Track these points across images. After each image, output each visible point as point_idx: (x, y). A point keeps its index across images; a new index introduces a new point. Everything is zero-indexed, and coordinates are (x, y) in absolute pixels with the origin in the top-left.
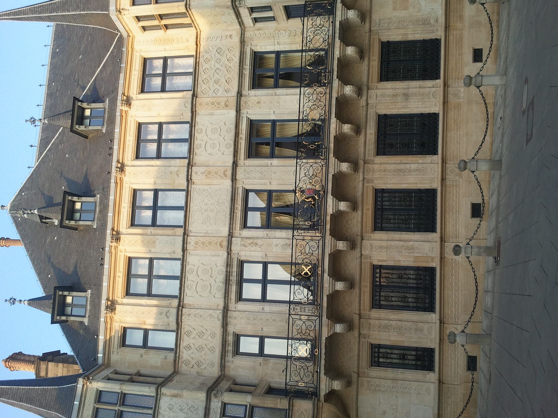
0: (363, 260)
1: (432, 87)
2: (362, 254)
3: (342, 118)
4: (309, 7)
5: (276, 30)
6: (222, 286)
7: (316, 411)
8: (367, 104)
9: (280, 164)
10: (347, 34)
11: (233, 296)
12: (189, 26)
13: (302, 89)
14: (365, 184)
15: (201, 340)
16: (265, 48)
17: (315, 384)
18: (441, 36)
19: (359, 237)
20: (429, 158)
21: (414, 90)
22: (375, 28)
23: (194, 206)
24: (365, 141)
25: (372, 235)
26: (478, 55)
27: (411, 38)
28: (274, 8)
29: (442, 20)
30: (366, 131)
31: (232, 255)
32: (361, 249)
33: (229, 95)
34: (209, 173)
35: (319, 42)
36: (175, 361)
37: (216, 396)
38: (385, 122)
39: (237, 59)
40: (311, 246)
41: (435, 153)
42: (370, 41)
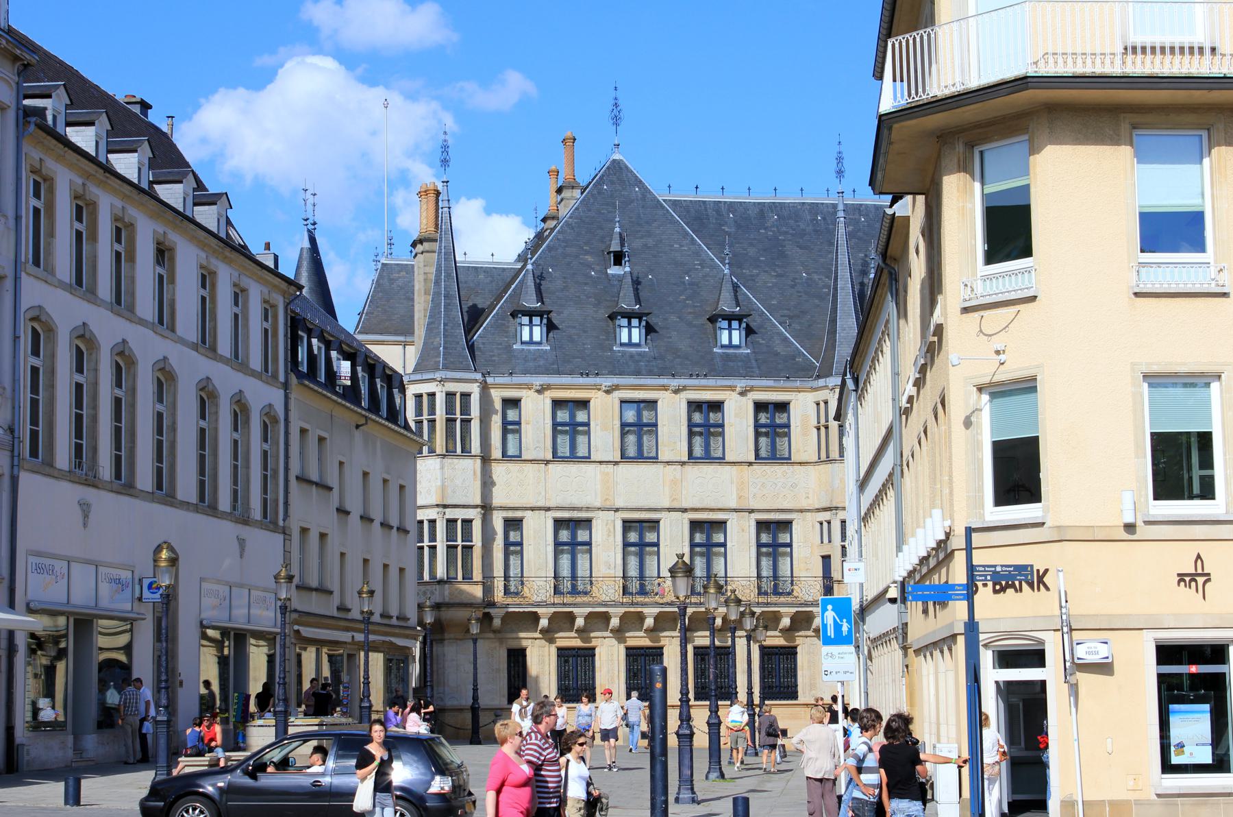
39: (786, 506)
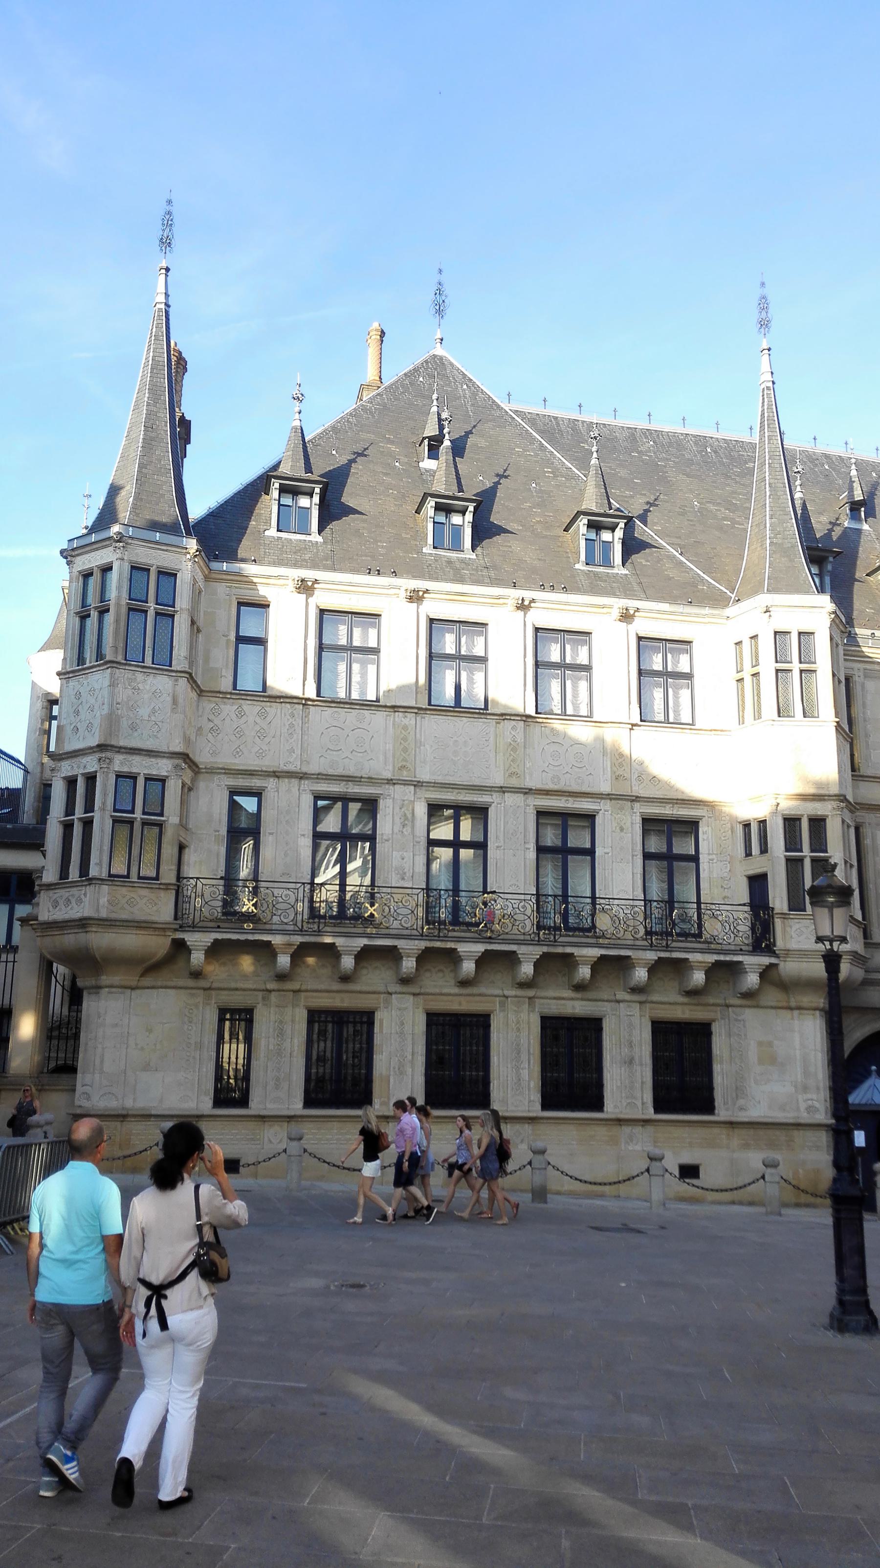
0: (382, 996)
1: (642, 1101)
2: (391, 994)
3: (601, 965)
4: (764, 914)
5: (731, 857)
6: (340, 771)
7: (161, 926)
8: (618, 1002)
9: (528, 862)
10: (724, 971)
11: (324, 787)
12: (741, 721)
13: (642, 903)
14: (498, 999)
15: (253, 733)
16: (704, 840)
17: (199, 925)
18: (719, 1115)
19: (417, 991)
20: (537, 1097)
21: (638, 1074)
22: (731, 1014)
23: (462, 724)
24: (563, 999)
25: (421, 1010)
26: (689, 1172)
27: (717, 1068)
28: (765, 857)
29: (743, 1117)
30: (577, 999)
31: (387, 786)
32: (400, 993)
33: (634, 782)
34: (514, 750)
35: (712, 928)
36: (220, 692)
37: (176, 767)
38: (591, 1028)
40: (401, 912)
41: (545, 1106)
42: (713, 1005)
